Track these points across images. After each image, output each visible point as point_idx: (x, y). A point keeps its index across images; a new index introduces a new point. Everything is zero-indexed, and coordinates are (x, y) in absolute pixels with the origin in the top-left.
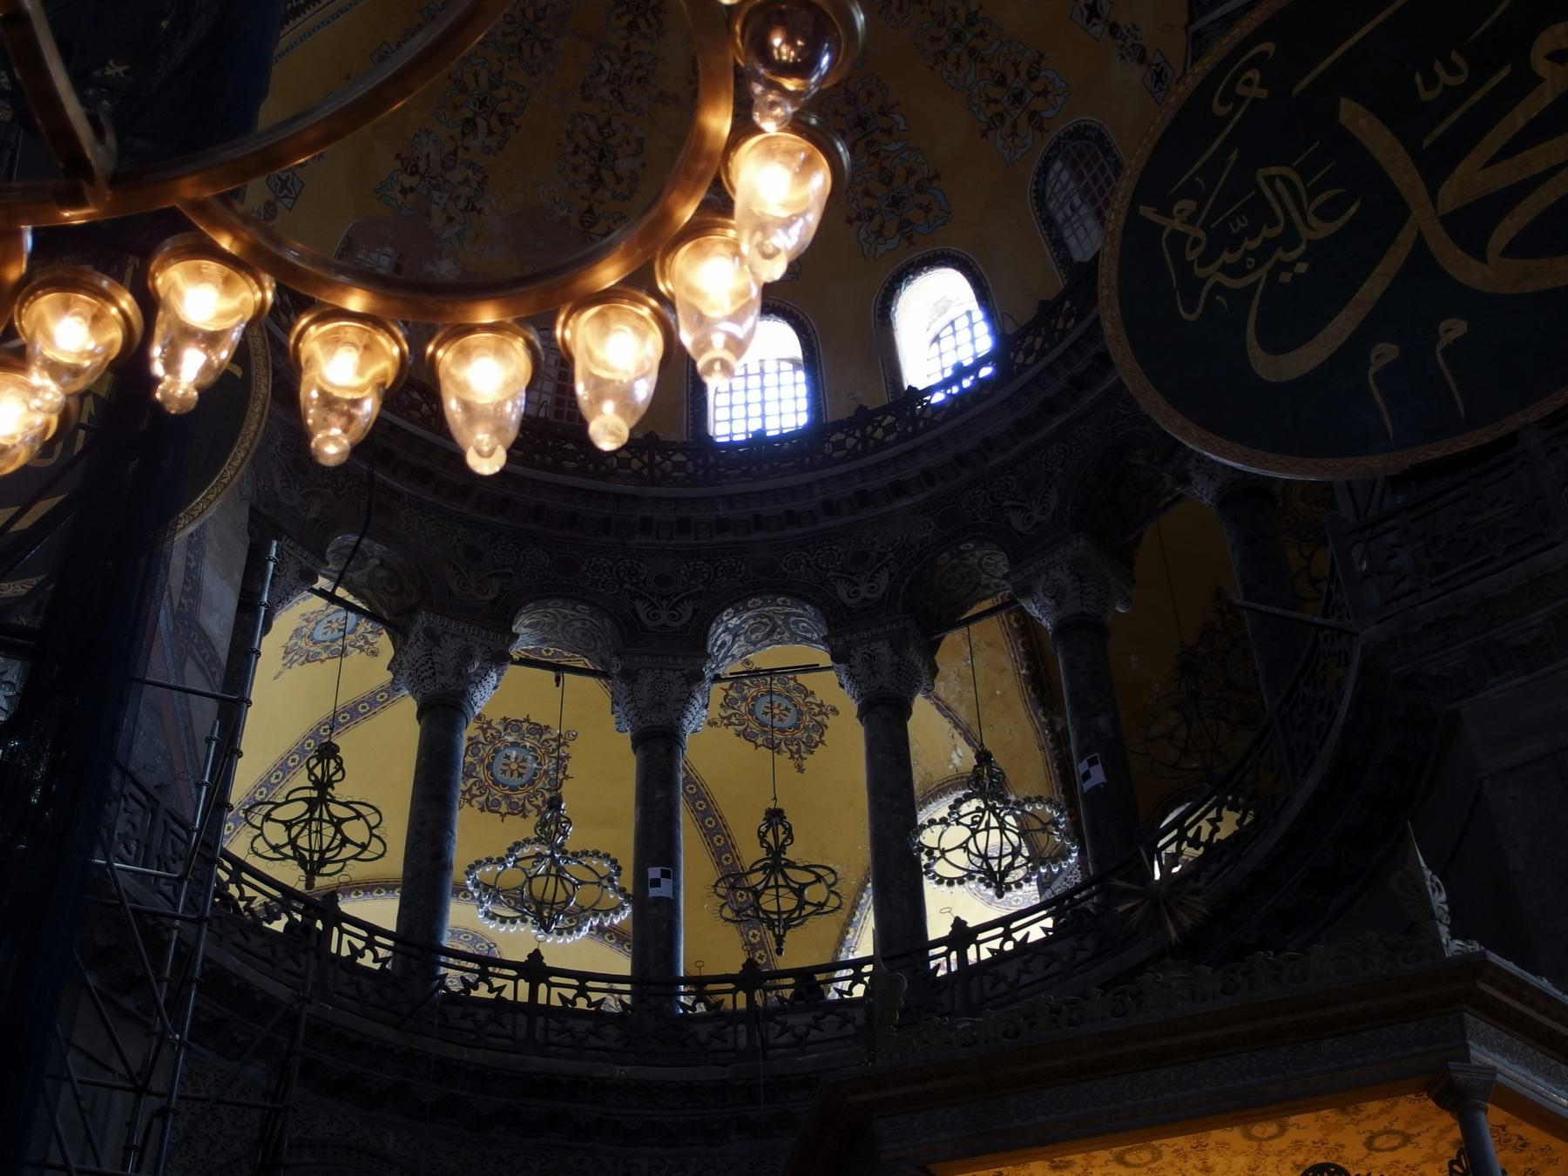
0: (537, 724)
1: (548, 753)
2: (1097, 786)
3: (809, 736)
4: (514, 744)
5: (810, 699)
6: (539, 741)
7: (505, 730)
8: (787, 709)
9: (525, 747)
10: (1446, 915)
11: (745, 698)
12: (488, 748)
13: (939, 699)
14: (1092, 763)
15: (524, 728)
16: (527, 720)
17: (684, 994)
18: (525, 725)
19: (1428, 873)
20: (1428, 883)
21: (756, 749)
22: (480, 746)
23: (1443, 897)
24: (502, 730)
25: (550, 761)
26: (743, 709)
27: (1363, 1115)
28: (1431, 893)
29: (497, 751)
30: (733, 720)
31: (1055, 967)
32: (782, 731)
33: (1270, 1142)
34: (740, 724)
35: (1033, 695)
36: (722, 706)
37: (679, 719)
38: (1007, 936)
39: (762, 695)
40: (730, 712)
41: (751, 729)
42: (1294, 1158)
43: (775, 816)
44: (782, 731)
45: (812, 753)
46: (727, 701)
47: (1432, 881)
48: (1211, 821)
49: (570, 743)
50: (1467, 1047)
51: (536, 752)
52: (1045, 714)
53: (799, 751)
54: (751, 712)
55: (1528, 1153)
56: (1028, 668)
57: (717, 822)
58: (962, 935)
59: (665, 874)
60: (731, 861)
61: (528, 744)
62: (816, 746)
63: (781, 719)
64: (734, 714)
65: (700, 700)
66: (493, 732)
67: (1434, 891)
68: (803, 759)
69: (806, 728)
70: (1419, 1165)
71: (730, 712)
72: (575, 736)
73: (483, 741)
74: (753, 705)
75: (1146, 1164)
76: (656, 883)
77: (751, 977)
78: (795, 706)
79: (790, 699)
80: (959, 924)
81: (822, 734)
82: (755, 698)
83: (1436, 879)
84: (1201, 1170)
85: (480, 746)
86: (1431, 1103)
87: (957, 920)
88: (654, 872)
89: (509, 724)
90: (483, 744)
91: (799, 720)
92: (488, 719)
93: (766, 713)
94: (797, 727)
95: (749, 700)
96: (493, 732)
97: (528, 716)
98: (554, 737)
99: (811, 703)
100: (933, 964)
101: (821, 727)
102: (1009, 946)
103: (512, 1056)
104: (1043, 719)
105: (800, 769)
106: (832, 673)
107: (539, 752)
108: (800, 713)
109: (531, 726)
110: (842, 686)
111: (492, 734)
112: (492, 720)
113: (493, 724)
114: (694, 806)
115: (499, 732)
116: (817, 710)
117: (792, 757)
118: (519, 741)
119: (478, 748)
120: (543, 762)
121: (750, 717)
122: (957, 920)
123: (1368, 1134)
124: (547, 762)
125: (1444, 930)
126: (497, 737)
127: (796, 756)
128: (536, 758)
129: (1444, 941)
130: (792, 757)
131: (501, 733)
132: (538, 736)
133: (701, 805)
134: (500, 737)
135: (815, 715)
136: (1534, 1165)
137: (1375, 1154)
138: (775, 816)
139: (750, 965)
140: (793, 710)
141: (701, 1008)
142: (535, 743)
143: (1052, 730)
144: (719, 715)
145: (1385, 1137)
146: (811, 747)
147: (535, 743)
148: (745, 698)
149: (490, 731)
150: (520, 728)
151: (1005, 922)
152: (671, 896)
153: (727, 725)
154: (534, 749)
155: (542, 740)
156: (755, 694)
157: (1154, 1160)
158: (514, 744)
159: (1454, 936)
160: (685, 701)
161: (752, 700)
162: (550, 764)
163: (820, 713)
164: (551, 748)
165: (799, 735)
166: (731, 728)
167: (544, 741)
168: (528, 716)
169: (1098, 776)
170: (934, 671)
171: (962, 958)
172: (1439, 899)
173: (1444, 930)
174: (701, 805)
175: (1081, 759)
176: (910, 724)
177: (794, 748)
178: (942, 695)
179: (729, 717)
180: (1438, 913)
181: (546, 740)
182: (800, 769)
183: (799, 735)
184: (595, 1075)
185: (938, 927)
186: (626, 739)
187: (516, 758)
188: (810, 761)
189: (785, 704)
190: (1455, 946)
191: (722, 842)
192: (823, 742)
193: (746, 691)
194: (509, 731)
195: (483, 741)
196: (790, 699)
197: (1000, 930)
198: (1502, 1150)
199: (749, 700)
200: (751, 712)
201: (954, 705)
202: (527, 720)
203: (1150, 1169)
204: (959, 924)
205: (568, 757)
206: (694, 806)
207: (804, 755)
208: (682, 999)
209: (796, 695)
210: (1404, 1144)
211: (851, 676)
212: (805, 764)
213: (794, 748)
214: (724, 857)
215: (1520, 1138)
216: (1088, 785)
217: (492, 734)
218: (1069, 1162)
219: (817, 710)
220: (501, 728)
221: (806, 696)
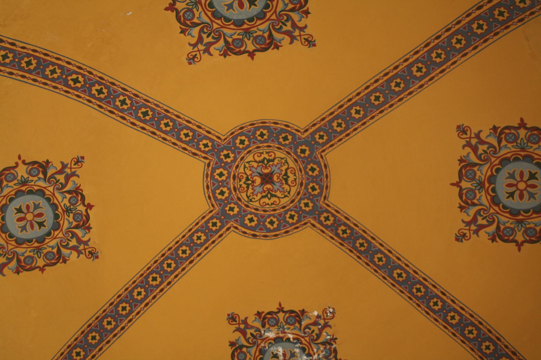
0: (292, 312)
1: (313, 340)
4: (278, 340)
6: (300, 329)
7: (263, 326)
9: (288, 339)
11: (481, 185)
12: (253, 350)
15: (281, 320)
16: (281, 309)
18: (281, 315)
21: (519, 250)
22: (244, 349)
24: (260, 327)
25: (318, 349)
26: (484, 201)
29: (262, 352)
30: (481, 221)
34: (491, 223)
39: (498, 170)
40: (473, 211)
41: (504, 223)
46: (464, 198)
49: (331, 323)
51: (301, 343)
54: (495, 201)
61: (291, 336)
64: (478, 212)
66: (252, 331)
71: (473, 211)
72: (333, 313)
73: (245, 343)
74: (494, 190)
82: (492, 179)
85: (244, 349)
89: (265, 318)
90: (247, 347)
92: (242, 318)
93: (511, 195)
95: (487, 185)
96: (252, 331)
97: (280, 305)
98: (312, 321)
107: (304, 342)
109: (288, 315)
111: (252, 334)
112: (246, 318)
113: (249, 322)
115: (258, 330)
118: (281, 335)
119: (244, 353)
120: (311, 352)
121: (496, 208)
124: (315, 350)
126: (257, 337)
128: (303, 350)
131: (260, 331)
132: (297, 325)
133: (488, 348)
134: (261, 336)
142: (298, 333)
144: (463, 221)
147: (298, 333)
148: (481, 185)
149: (249, 331)
150: (277, 321)
153: (476, 232)
154: (298, 340)
155: (302, 328)
156: (489, 173)
158: (278, 340)
161: (490, 183)
162: (320, 352)
164: (314, 334)
166: (482, 233)
167: (305, 328)
168: (280, 305)
179: (474, 220)
181: (307, 327)
187: (284, 355)
193: (478, 173)
194: (267, 326)
195: (245, 343)
199: (487, 185)
200: (495, 201)
202: (281, 309)
205: (334, 339)
217: (252, 334)
220: (258, 324)
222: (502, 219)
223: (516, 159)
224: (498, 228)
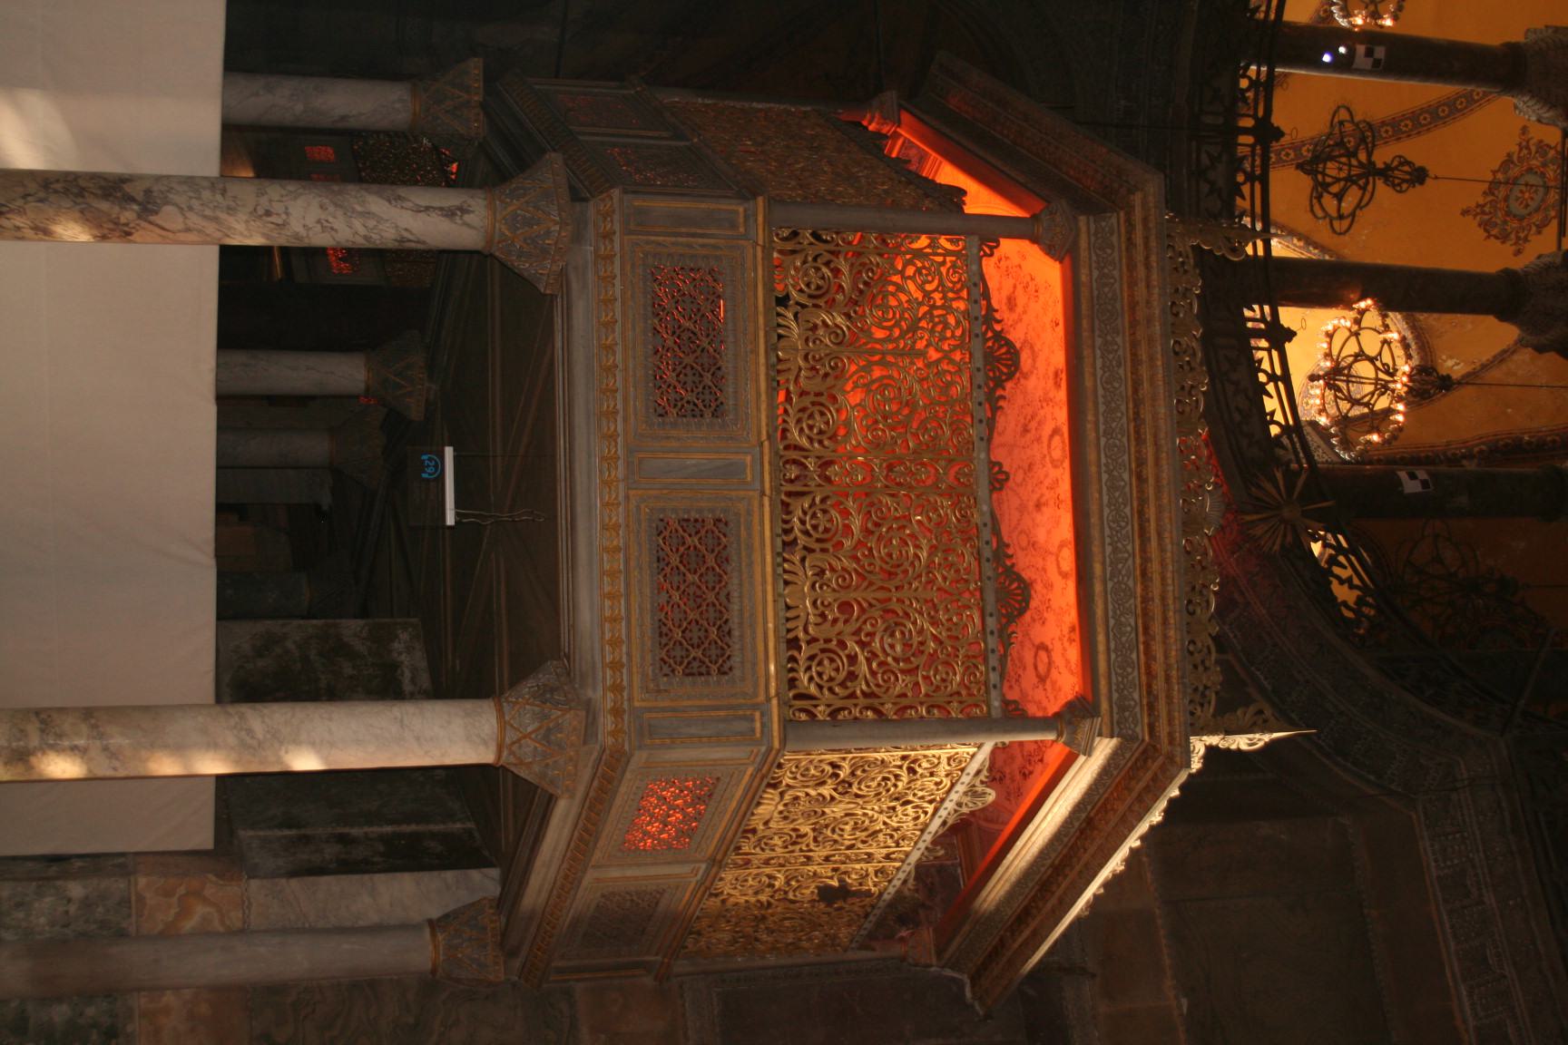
2: (1401, 484)
3: (1496, 224)
5: (1534, 229)
8: (1527, 206)
10: (1227, 745)
11: (1544, 165)
13: (1514, 352)
14: (1424, 484)
17: (1258, 71)
19: (1267, 738)
20: (1257, 736)
23: (1244, 747)
26: (1534, 162)
27: (1066, 644)
28: (1251, 736)
30: (1525, 151)
31: (1237, 417)
32: (1506, 199)
33: (1055, 563)
34: (1519, 157)
35: (1501, 443)
36: (1541, 141)
37: (1530, 91)
38: (1272, 377)
40: (1533, 149)
42: (1039, 581)
43: (1419, 176)
44: (1506, 199)
45: (1480, 225)
47: (1259, 740)
48: (1349, 580)
50: (1112, 737)
52: (1481, 452)
53: (1483, 213)
54: (1530, 170)
55: (1018, 777)
56: (1529, 443)
57: (1425, 125)
58: (1279, 336)
59: (1377, 63)
60: (1384, 135)
62: (1485, 230)
63: (1517, 199)
64: (1530, 153)
65: (1546, 115)
67: (1250, 739)
68: (1475, 216)
69: (1505, 222)
70: (1019, 686)
71: (1533, 149)
75: (1049, 453)
76: (1369, 53)
77: (1267, 133)
78: (1530, 214)
79: (1537, 210)
80: (1290, 335)
81: (1497, 238)
82: (1543, 175)
83: (1261, 744)
84: (1038, 500)
86: (1070, 697)
87: (1294, 334)
88: (1380, 52)
91: (1515, 216)
94: (1508, 213)
99: (1530, 230)
100: (1256, 307)
101: (1503, 238)
102: (1262, 378)
104: (1476, 450)
105: (1465, 213)
106: (1554, 249)
108: (1521, 219)
110: (1539, 257)
114: (1444, 105)
116: (1522, 235)
117: (1478, 206)
122: (1294, 334)
123: (1050, 647)
125: (1214, 740)
127: (1478, 210)
129: (1205, 738)
130: (1478, 206)
133: (1443, 111)
135: (1517, 232)
136: (1008, 781)
137: (1034, 650)
138: (1419, 176)
139: (1278, 134)
140: (1525, 212)
141: (1244, 83)
143: (1464, 457)
145: (1046, 660)
146: (1485, 226)
148: (1544, 165)
151: (1286, 378)
152: (1354, 66)
153: (1520, 145)
157: (1052, 461)
159: (1211, 750)
160: (1547, 100)
163: (1518, 238)
165: (1499, 214)
166: (1517, 148)
169: (1411, 487)
170: (1540, 349)
171: (1258, 334)
172: (1241, 742)
173: (1214, 740)
174: (1443, 111)
175: (1429, 473)
176: (1491, 320)
177: (1487, 209)
178: (1516, 357)
179: (1528, 148)
180: (1231, 738)
182: (1465, 213)
183: (1499, 214)
185: (1289, 316)
186: (1517, 36)
188: (1472, 223)
189: (1533, 205)
190: (1199, 745)
191: (1404, 129)
192: (1488, 237)
196: (1537, 210)
197: (1278, 371)
198: (1023, 756)
200: (1530, 170)
201: (1504, 367)
203: (1045, 456)
204: (1290, 335)
206: (1444, 105)
207: (1478, 218)
208: (1254, 68)
209: (1537, 218)
210: (1038, 676)
211: (1548, 268)
212: (1469, 218)
213: (1487, 209)
214: (1389, 128)
215: (1031, 773)
216: (1403, 475)
218: (1060, 386)
219: (1522, 235)
221: (1537, 226)
222: (1516, 169)
223: (1543, 200)
224: (1513, 162)
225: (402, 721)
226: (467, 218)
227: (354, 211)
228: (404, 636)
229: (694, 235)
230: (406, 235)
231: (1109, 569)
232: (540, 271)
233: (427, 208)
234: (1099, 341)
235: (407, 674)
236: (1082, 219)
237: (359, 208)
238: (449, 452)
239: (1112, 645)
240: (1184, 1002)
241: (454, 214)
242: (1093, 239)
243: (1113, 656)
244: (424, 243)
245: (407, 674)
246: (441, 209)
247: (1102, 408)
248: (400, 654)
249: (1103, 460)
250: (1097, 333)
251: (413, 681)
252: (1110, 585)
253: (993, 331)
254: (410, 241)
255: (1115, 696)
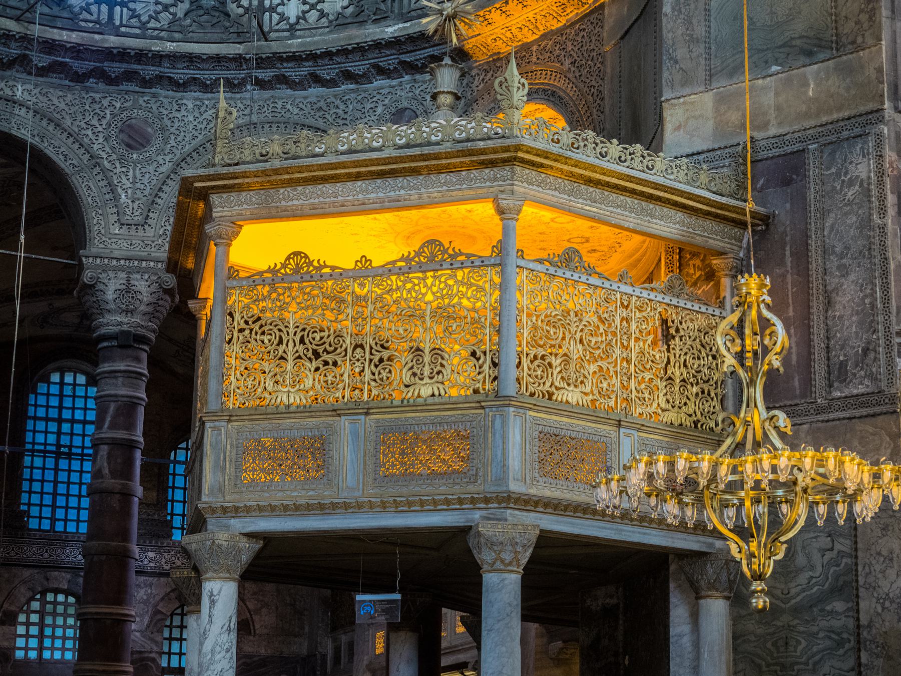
103: (97, 37)
184: (153, 49)
225: (489, 631)
226: (215, 593)
227: (211, 659)
228: (589, 602)
229: (225, 458)
230: (225, 628)
231: (414, 191)
232: (248, 550)
233: (210, 616)
234: (283, 203)
235: (608, 601)
236: (214, 215)
237: (209, 656)
238: (359, 597)
239: (458, 187)
240: (775, 68)
241: (213, 601)
242: (226, 209)
243: (464, 186)
244: (231, 617)
245: (608, 601)
246: (210, 608)
247: (321, 199)
248: (598, 605)
249: (351, 197)
250: (278, 204)
251: (611, 597)
252: (423, 190)
253: (281, 269)
254: (229, 626)
255: (488, 184)
